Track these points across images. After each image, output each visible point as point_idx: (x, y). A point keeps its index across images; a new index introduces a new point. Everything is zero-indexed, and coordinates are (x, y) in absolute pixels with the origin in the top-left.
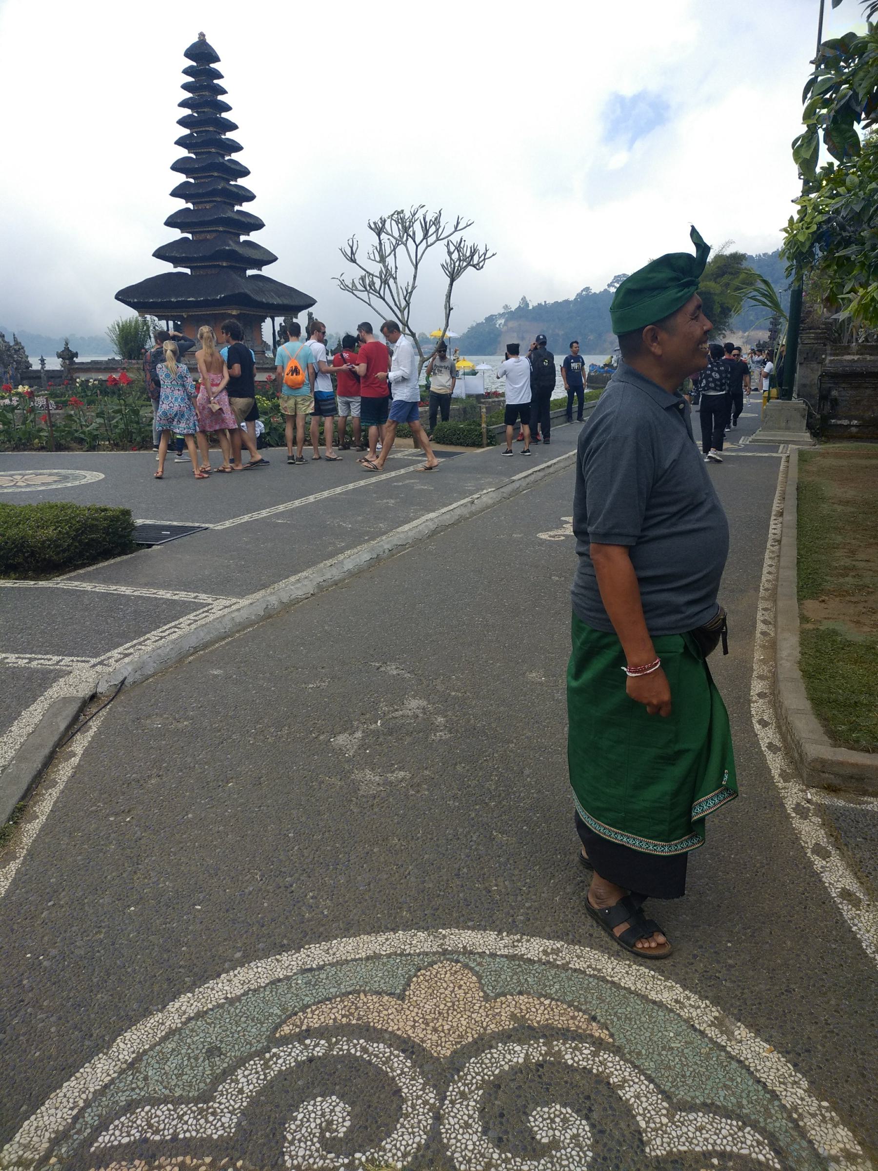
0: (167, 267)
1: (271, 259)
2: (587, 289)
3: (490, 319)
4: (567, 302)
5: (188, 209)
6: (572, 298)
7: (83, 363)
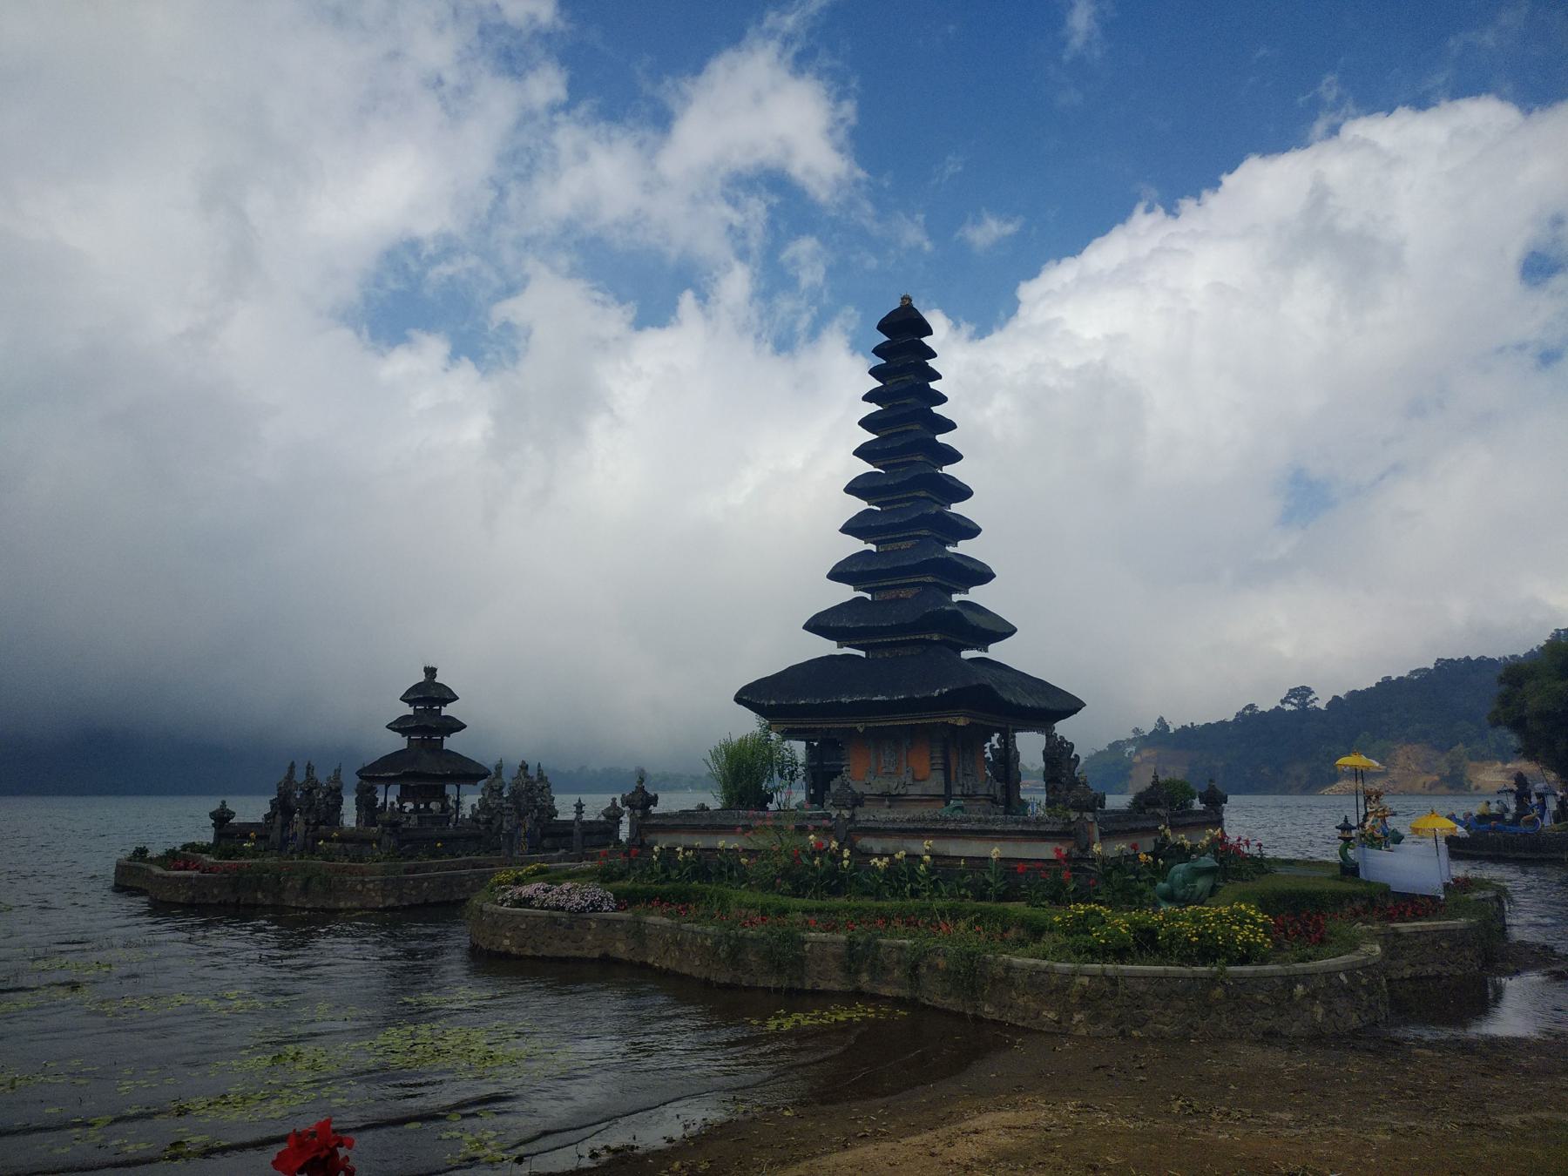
0: (827, 647)
1: (1003, 631)
2: (1251, 706)
3: (1116, 747)
4: (1223, 724)
6: (1231, 718)
7: (664, 816)
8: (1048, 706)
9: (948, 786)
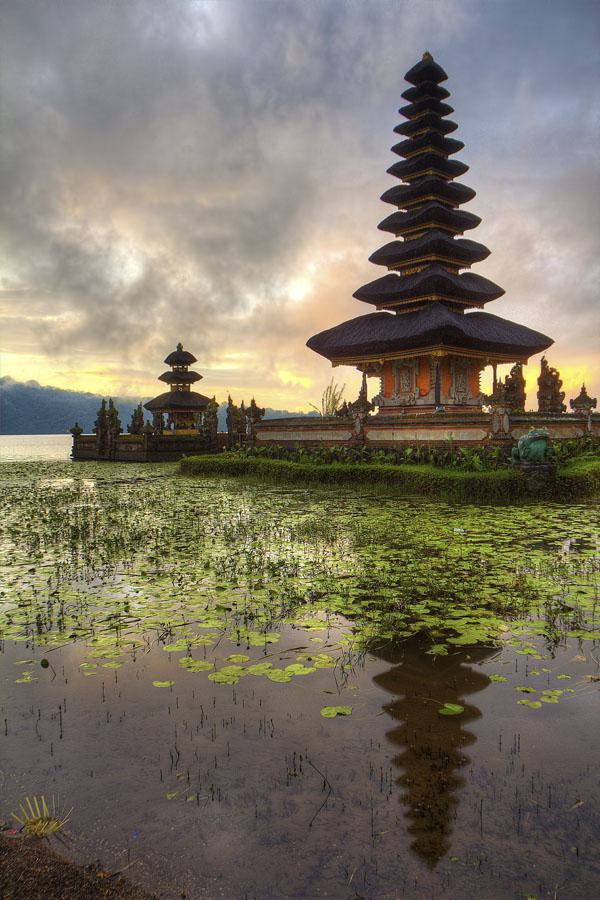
0: (370, 309)
5: (396, 244)
8: (523, 343)
9: (437, 397)
